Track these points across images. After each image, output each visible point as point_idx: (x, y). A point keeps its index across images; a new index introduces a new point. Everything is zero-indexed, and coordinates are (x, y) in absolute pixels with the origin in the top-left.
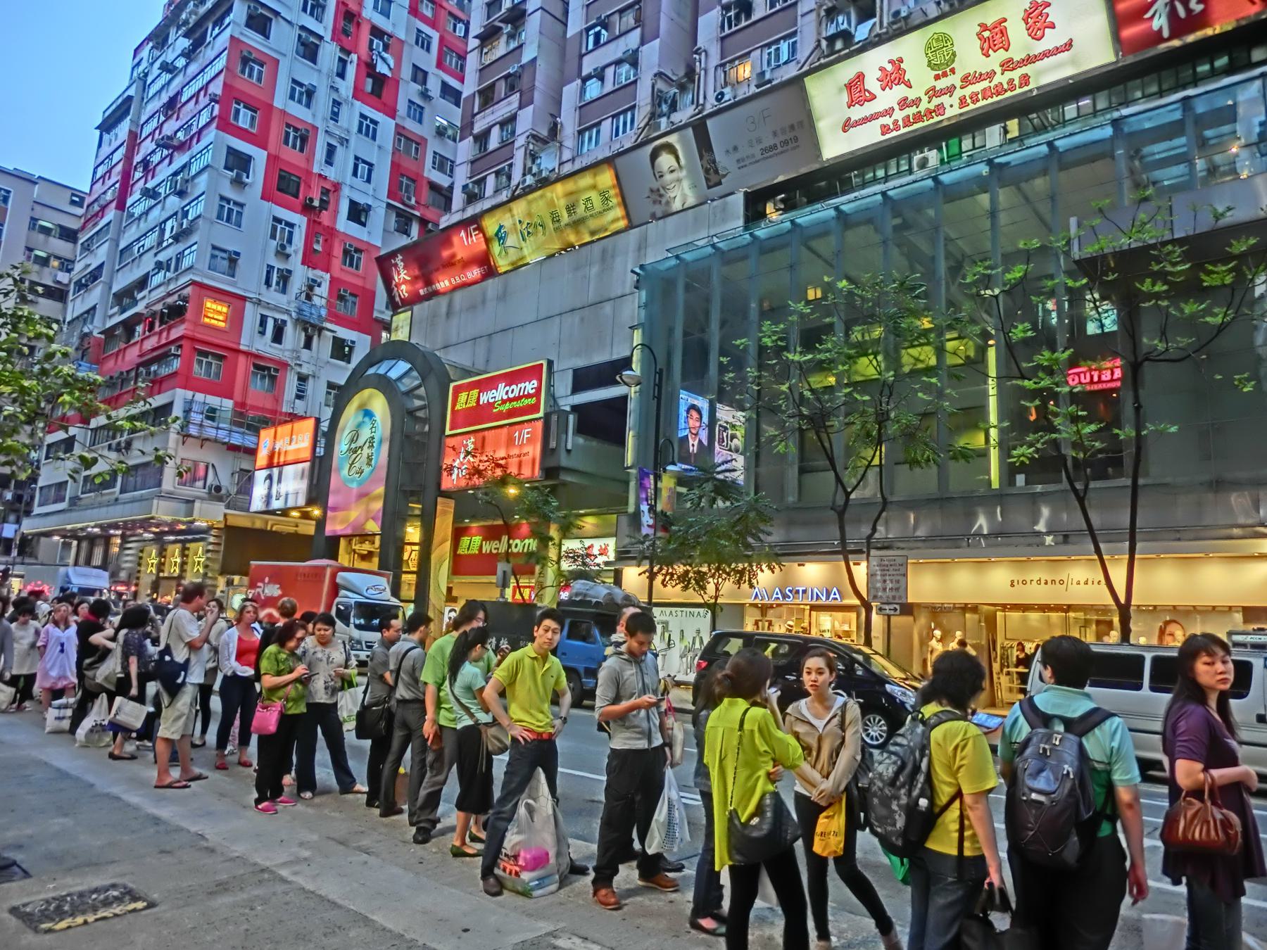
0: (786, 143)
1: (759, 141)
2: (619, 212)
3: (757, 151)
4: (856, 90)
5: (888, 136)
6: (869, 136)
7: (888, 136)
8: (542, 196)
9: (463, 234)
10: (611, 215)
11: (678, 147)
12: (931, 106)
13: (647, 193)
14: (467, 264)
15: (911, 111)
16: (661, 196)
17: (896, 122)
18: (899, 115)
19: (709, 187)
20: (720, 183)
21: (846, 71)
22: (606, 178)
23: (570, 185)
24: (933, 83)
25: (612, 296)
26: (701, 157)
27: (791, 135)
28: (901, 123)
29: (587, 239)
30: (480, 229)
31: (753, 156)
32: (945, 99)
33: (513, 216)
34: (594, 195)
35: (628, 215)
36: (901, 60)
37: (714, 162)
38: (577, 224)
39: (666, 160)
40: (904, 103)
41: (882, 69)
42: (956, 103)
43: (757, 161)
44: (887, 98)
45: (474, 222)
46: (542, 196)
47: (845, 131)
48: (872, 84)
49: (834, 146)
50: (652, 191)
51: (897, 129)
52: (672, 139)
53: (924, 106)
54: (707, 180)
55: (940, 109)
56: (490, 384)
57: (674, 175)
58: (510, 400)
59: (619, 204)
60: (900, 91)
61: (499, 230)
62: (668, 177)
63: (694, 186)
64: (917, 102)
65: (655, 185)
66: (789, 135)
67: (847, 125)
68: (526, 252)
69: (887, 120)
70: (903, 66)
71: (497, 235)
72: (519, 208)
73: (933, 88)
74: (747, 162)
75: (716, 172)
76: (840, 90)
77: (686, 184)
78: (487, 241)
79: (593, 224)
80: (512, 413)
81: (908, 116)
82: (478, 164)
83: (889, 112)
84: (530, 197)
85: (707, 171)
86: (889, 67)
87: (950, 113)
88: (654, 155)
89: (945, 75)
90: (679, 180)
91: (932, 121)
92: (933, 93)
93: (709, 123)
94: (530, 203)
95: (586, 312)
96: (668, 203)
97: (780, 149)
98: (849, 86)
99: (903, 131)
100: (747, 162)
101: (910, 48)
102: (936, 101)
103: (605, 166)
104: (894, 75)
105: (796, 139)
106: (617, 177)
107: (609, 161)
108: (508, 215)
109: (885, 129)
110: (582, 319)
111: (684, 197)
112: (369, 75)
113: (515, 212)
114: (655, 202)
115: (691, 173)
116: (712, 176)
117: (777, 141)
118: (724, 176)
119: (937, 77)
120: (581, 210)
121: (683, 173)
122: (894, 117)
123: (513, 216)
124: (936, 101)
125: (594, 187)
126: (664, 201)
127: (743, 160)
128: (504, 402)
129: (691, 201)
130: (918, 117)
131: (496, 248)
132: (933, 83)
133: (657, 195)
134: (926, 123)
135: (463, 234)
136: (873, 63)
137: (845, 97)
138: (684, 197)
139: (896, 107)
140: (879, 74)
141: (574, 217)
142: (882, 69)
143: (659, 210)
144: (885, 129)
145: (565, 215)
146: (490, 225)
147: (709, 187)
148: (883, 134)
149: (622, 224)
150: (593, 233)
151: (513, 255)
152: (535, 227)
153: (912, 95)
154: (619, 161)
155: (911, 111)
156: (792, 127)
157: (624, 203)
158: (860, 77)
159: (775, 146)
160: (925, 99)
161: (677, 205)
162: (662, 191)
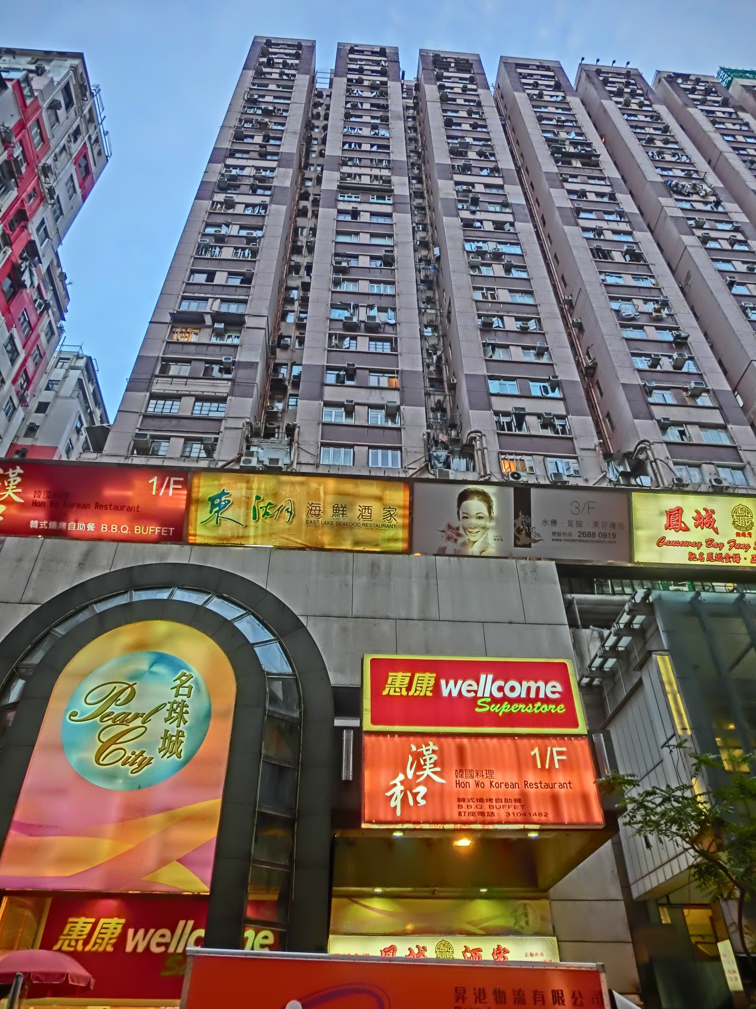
0: (604, 535)
1: (579, 524)
2: (401, 534)
3: (575, 532)
4: (674, 517)
5: (693, 563)
6: (677, 557)
7: (693, 563)
8: (302, 483)
9: (155, 480)
10: (390, 533)
11: (493, 498)
12: (731, 553)
13: (444, 527)
14: (140, 515)
15: (715, 551)
16: (459, 535)
17: (701, 554)
18: (705, 550)
19: (516, 545)
20: (529, 546)
21: (672, 501)
22: (398, 497)
23: (348, 486)
24: (735, 537)
25: (392, 615)
26: (516, 516)
27: (611, 531)
28: (705, 556)
29: (348, 546)
30: (187, 485)
31: (570, 534)
32: (741, 552)
33: (249, 489)
34: (376, 508)
35: (410, 540)
36: (713, 512)
37: (529, 525)
38: (339, 527)
39: (475, 505)
40: (710, 543)
41: (697, 512)
42: (749, 558)
43: (574, 541)
44: (698, 534)
45: (184, 476)
46: (302, 483)
47: (658, 545)
48: (688, 518)
49: (646, 554)
50: (449, 527)
51: (702, 559)
52: (489, 490)
53: (725, 551)
54: (516, 538)
55: (737, 557)
56: (471, 671)
57: (481, 522)
58: (512, 701)
59: (403, 527)
60: (708, 533)
61: (219, 496)
62: (474, 521)
63: (498, 539)
64: (720, 546)
65: (455, 523)
66: (608, 530)
67: (661, 542)
68: (251, 532)
69: (694, 550)
70: (714, 516)
71: (212, 500)
72: (262, 484)
73: (734, 541)
74: (562, 538)
75: (529, 535)
76: (661, 514)
77: (491, 535)
78: (189, 501)
79: (362, 534)
80: (510, 719)
81: (712, 554)
82: (149, 421)
83: (698, 545)
84: (284, 478)
85: (518, 531)
86: (703, 513)
87: (743, 563)
88: (464, 497)
89: (744, 535)
90: (485, 528)
91: (729, 564)
92: (733, 544)
93: (533, 491)
94: (281, 483)
95: (350, 624)
96: (464, 544)
97: (597, 538)
98: (669, 514)
99: (706, 563)
100: (562, 538)
101: (722, 507)
102: (734, 551)
103: (402, 485)
104: (705, 520)
105: (614, 536)
106: (411, 503)
107: (409, 483)
108: (244, 485)
109: (692, 556)
110: (344, 630)
111: (486, 544)
112: (9, 276)
113: (255, 485)
114: (449, 538)
115: (500, 525)
116: (523, 535)
117: (596, 531)
118: (536, 541)
119: (738, 535)
120: (354, 514)
121: (492, 524)
122: (700, 550)
123: (249, 489)
124: (734, 551)
125: (380, 499)
126: (460, 540)
127: (559, 534)
128: (494, 700)
129: (491, 551)
130: (719, 557)
131: (201, 514)
132: (735, 537)
133: (454, 533)
134: (724, 564)
135: (155, 480)
136: (691, 505)
137: (664, 520)
138: (486, 544)
139: (704, 543)
140: (695, 515)
141: (341, 519)
142: (697, 512)
143: (450, 547)
144: (692, 556)
145: (330, 511)
146: (205, 487)
147: (516, 545)
148: (690, 559)
149: (400, 546)
150: (357, 543)
151: (227, 529)
152: (280, 510)
153: (718, 539)
154: (418, 486)
155: (715, 551)
156: (613, 525)
157: (410, 527)
158: (679, 511)
159: (594, 534)
160: (727, 546)
161: (475, 550)
162: (461, 531)
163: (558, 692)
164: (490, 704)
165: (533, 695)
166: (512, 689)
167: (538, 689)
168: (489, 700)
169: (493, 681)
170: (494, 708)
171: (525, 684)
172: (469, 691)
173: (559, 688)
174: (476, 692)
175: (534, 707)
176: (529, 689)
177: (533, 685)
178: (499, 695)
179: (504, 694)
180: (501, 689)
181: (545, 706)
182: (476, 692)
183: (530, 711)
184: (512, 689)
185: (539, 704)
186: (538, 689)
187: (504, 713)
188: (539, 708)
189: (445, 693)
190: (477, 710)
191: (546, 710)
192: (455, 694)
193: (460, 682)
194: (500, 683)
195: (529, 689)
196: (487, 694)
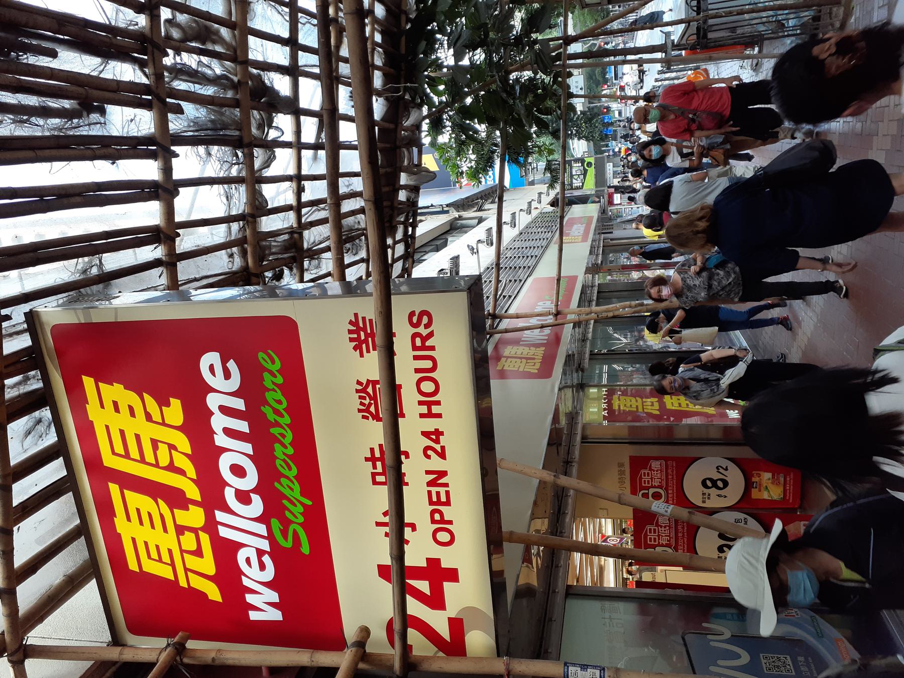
163: (224, 362)
164: (286, 523)
165: (243, 426)
166: (239, 471)
167: (224, 410)
168: (275, 523)
169: (228, 510)
170: (296, 513)
171: (221, 440)
172: (262, 567)
173: (210, 359)
174: (260, 553)
175: (277, 424)
176: (228, 432)
177: (219, 422)
178: (257, 506)
179: (254, 491)
180: (243, 497)
181: (269, 396)
182: (260, 553)
183: (289, 436)
184: (239, 471)
185: (267, 410)
186: (224, 410)
187: (303, 494)
188: (277, 412)
189: (275, 615)
190: (306, 549)
191: (279, 395)
192: (274, 597)
193: (246, 582)
194: (229, 495)
195: (228, 432)
196: (262, 529)
